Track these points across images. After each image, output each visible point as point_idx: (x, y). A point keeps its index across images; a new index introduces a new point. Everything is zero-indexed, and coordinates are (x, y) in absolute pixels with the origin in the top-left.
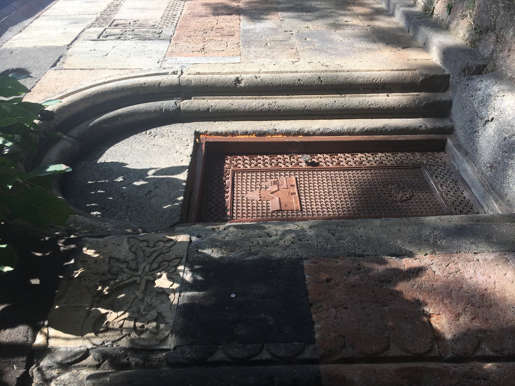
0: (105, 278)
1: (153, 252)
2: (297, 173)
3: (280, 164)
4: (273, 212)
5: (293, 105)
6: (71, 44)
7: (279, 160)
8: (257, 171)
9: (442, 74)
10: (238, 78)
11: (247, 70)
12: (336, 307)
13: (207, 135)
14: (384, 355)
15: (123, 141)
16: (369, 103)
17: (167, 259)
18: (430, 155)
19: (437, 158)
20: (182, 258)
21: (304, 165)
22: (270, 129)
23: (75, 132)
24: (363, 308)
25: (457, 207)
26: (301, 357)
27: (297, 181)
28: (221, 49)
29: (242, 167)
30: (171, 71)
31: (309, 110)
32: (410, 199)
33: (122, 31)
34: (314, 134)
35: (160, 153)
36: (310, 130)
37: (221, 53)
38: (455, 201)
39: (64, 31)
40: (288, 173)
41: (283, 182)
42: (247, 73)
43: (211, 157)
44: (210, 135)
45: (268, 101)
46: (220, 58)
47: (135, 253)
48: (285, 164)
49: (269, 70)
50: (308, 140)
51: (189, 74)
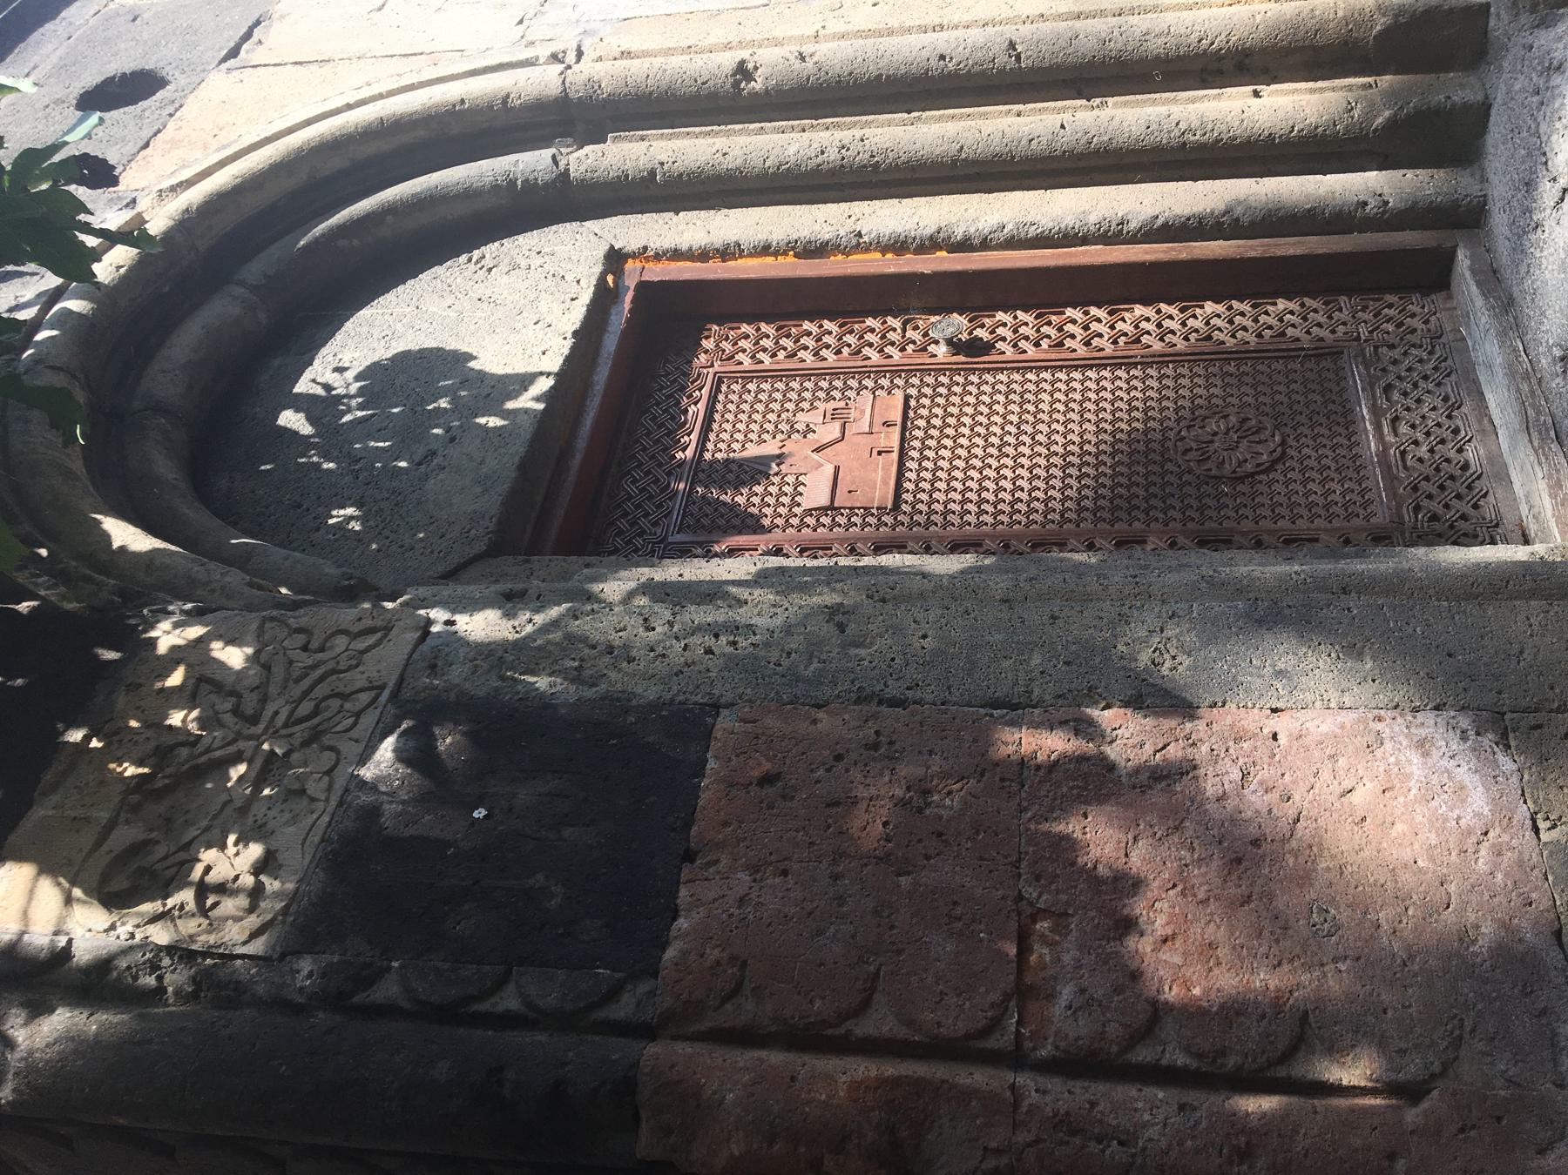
1: (314, 667)
3: (866, 351)
4: (809, 512)
8: (789, 375)
10: (742, 62)
11: (779, 33)
12: (754, 869)
13: (647, 259)
14: (842, 1030)
15: (401, 288)
16: (1183, 126)
17: (341, 689)
18: (1390, 306)
19: (1413, 315)
20: (382, 687)
21: (941, 350)
22: (842, 233)
23: (255, 270)
25: (1425, 503)
29: (747, 363)
30: (544, 52)
31: (975, 162)
32: (1271, 468)
34: (985, 244)
36: (972, 230)
38: (1427, 479)
40: (885, 382)
41: (863, 412)
42: (778, 43)
44: (658, 257)
45: (838, 135)
47: (267, 667)
48: (881, 351)
49: (850, 28)
50: (959, 267)
51: (600, 59)
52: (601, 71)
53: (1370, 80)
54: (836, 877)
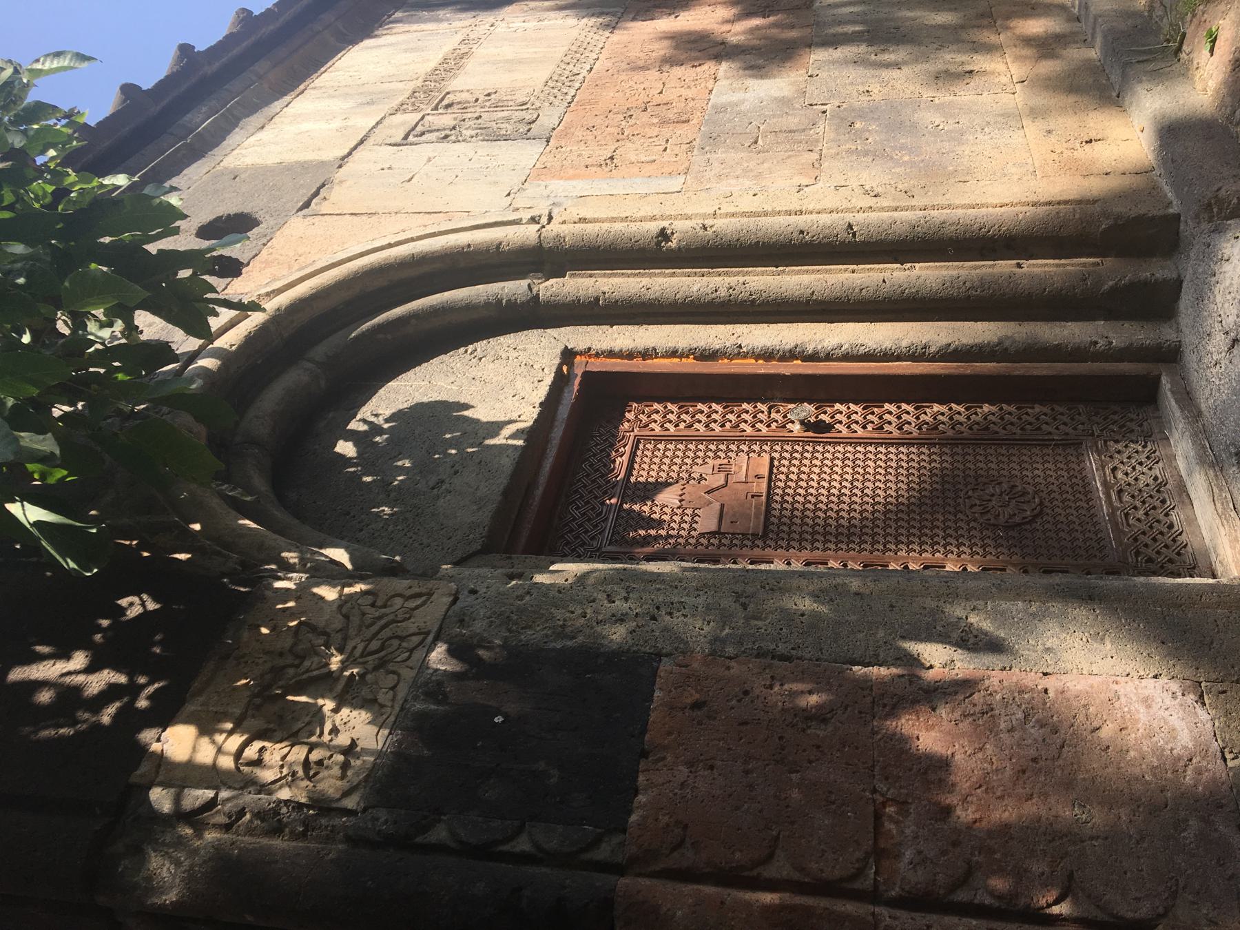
0: (280, 662)
2: (778, 448)
3: (743, 425)
4: (702, 535)
5: (783, 289)
6: (350, 154)
7: (744, 416)
8: (687, 440)
9: (1161, 213)
10: (664, 229)
11: (689, 211)
12: (690, 764)
13: (590, 356)
14: (754, 873)
15: (418, 369)
17: (399, 633)
18: (1115, 413)
19: (1132, 420)
20: (428, 633)
21: (796, 428)
22: (728, 345)
23: (320, 351)
24: (747, 772)
25: (1143, 549)
26: (587, 856)
27: (772, 465)
28: (648, 159)
29: (658, 430)
30: (526, 216)
31: (822, 302)
33: (455, 119)
34: (828, 357)
35: (503, 386)
37: (648, 169)
38: (1144, 533)
39: (344, 123)
40: (756, 448)
42: (688, 217)
43: (592, 405)
44: (597, 355)
45: (727, 279)
46: (639, 180)
47: (346, 617)
48: (753, 426)
49: (738, 210)
50: (810, 372)
51: (564, 222)
52: (563, 229)
53: (1098, 260)
54: (747, 772)
